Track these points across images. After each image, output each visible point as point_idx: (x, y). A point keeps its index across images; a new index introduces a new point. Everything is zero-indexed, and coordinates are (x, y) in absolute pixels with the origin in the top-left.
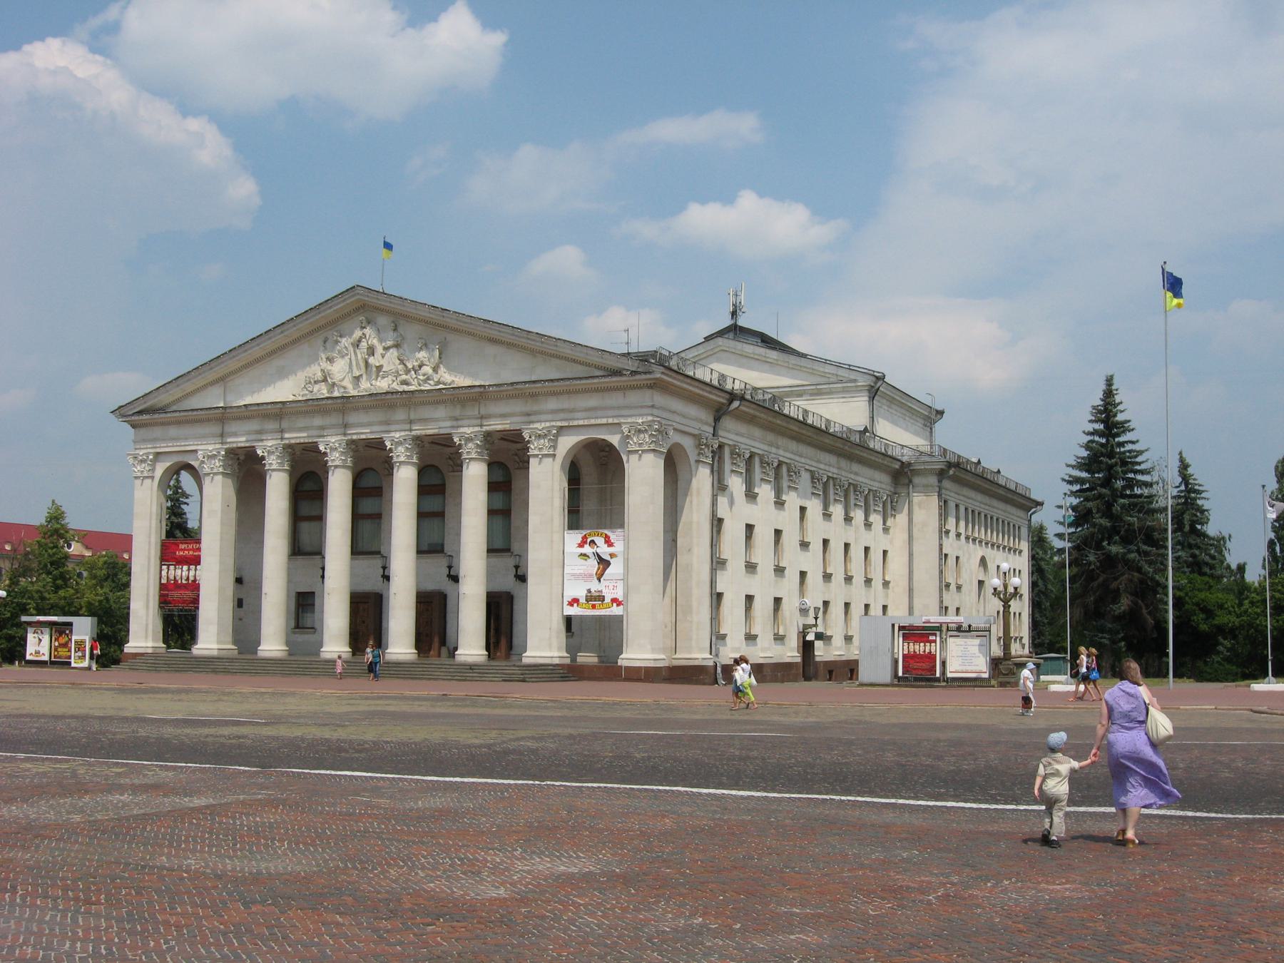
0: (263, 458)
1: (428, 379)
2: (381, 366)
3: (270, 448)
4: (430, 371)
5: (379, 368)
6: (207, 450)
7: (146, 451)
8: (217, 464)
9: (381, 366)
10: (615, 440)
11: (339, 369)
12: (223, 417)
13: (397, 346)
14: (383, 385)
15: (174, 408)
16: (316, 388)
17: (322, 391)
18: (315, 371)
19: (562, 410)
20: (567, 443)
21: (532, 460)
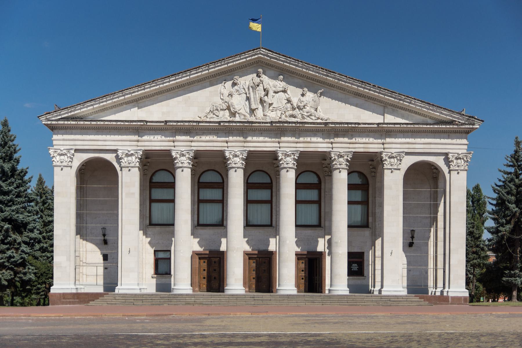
0: (176, 158)
1: (311, 115)
2: (272, 104)
4: (313, 111)
5: (271, 105)
8: (135, 161)
9: (272, 104)
10: (440, 162)
11: (239, 103)
13: (285, 91)
15: (91, 117)
16: (222, 112)
17: (225, 116)
19: (408, 143)
20: (409, 161)
21: (386, 171)
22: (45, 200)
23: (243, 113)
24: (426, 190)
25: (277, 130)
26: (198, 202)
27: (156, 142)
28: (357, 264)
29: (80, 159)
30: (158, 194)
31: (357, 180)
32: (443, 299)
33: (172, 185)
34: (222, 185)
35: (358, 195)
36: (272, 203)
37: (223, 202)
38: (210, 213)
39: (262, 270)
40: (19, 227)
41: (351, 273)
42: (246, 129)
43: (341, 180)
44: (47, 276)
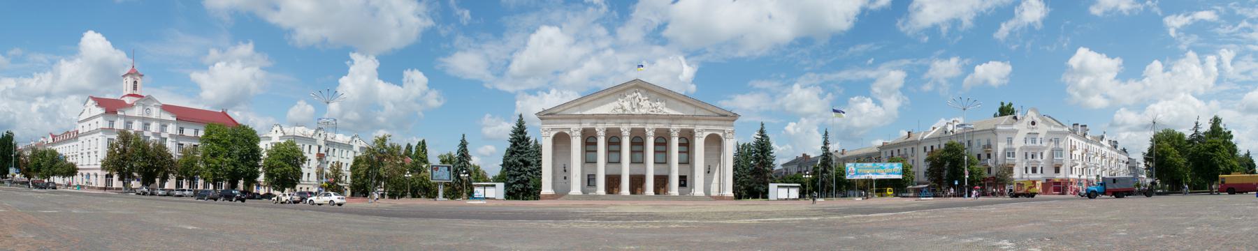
3: (600, 129)
6: (575, 130)
7: (546, 127)
8: (578, 133)
10: (721, 134)
11: (627, 105)
12: (581, 118)
14: (643, 111)
18: (616, 104)
22: (538, 151)
23: (629, 110)
24: (716, 147)
25: (646, 117)
26: (609, 152)
27: (587, 125)
28: (683, 181)
29: (553, 134)
30: (590, 148)
31: (684, 141)
32: (721, 198)
33: (596, 144)
34: (619, 143)
35: (684, 149)
36: (643, 152)
37: (619, 151)
38: (614, 157)
39: (637, 183)
40: (527, 164)
41: (680, 185)
42: (629, 117)
43: (675, 142)
44: (538, 186)
